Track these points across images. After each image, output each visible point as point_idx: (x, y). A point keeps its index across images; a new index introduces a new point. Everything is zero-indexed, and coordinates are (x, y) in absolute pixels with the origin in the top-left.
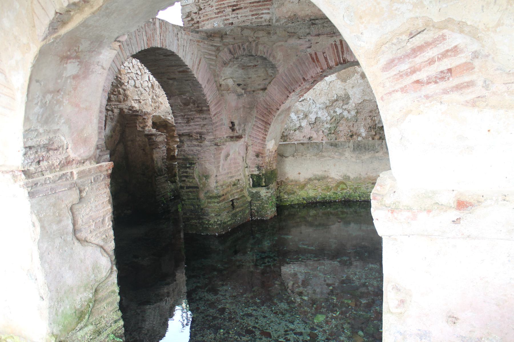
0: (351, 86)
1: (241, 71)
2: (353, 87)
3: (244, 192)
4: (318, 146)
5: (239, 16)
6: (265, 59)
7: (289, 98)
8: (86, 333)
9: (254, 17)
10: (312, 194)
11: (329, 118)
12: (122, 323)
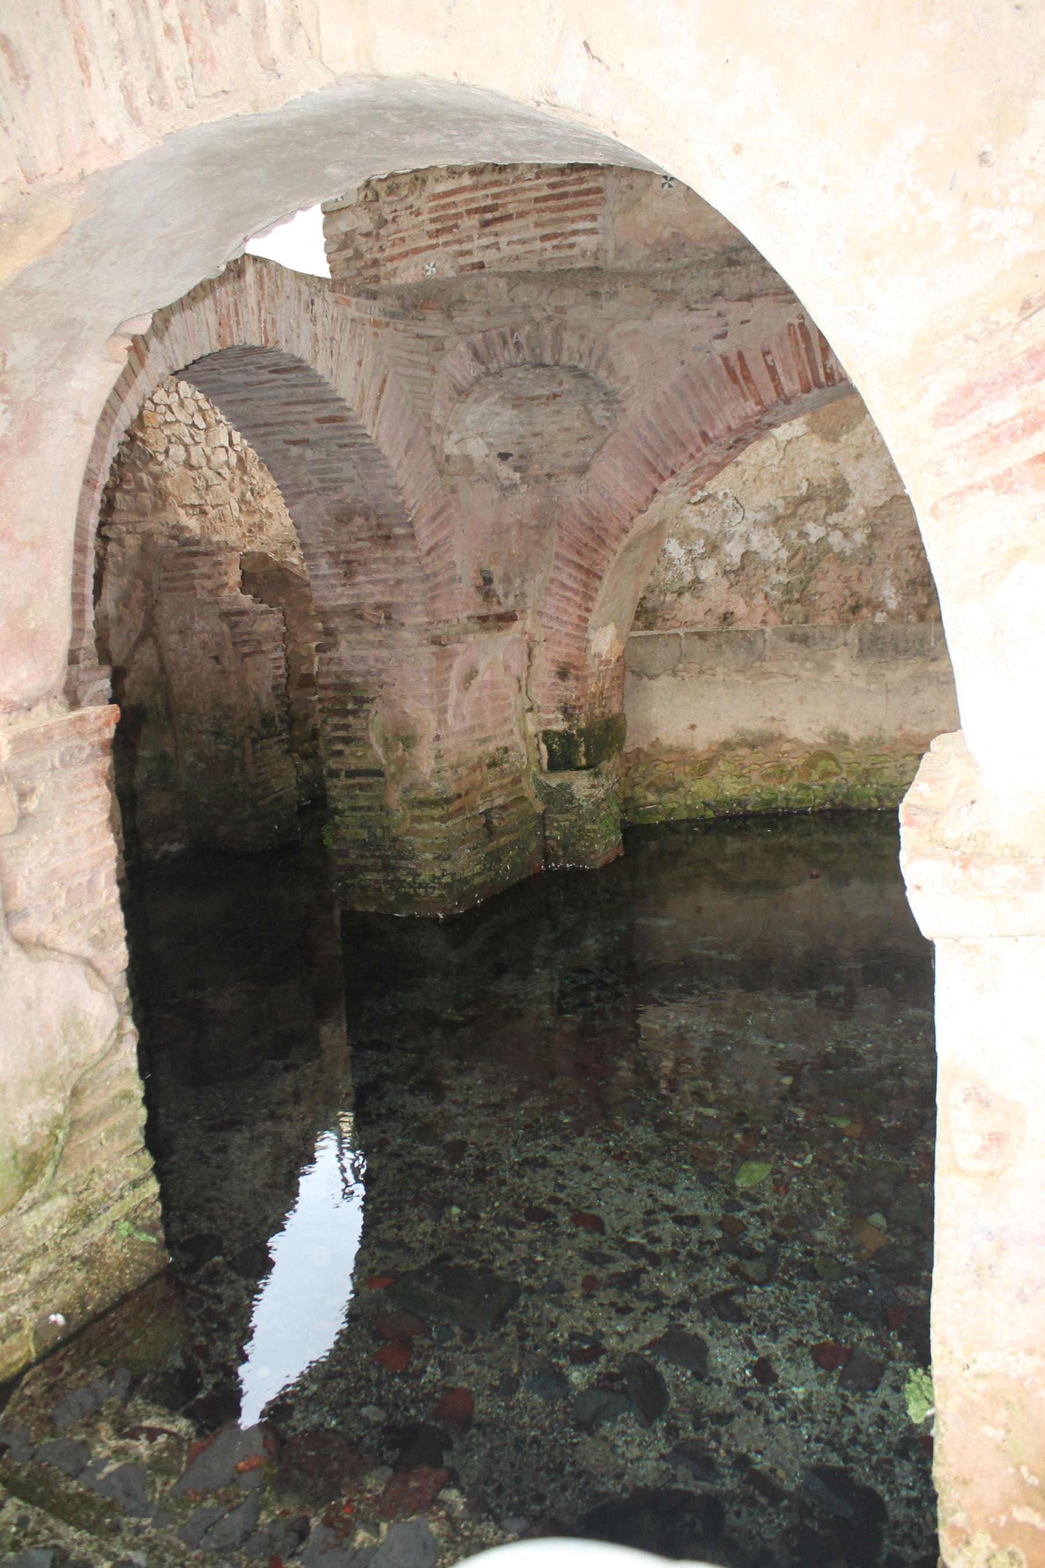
0: (853, 452)
1: (509, 414)
2: (859, 457)
3: (524, 784)
4: (751, 642)
5: (503, 240)
6: (584, 375)
7: (660, 499)
8: (49, 1220)
9: (548, 244)
10: (731, 788)
11: (784, 554)
12: (153, 1187)
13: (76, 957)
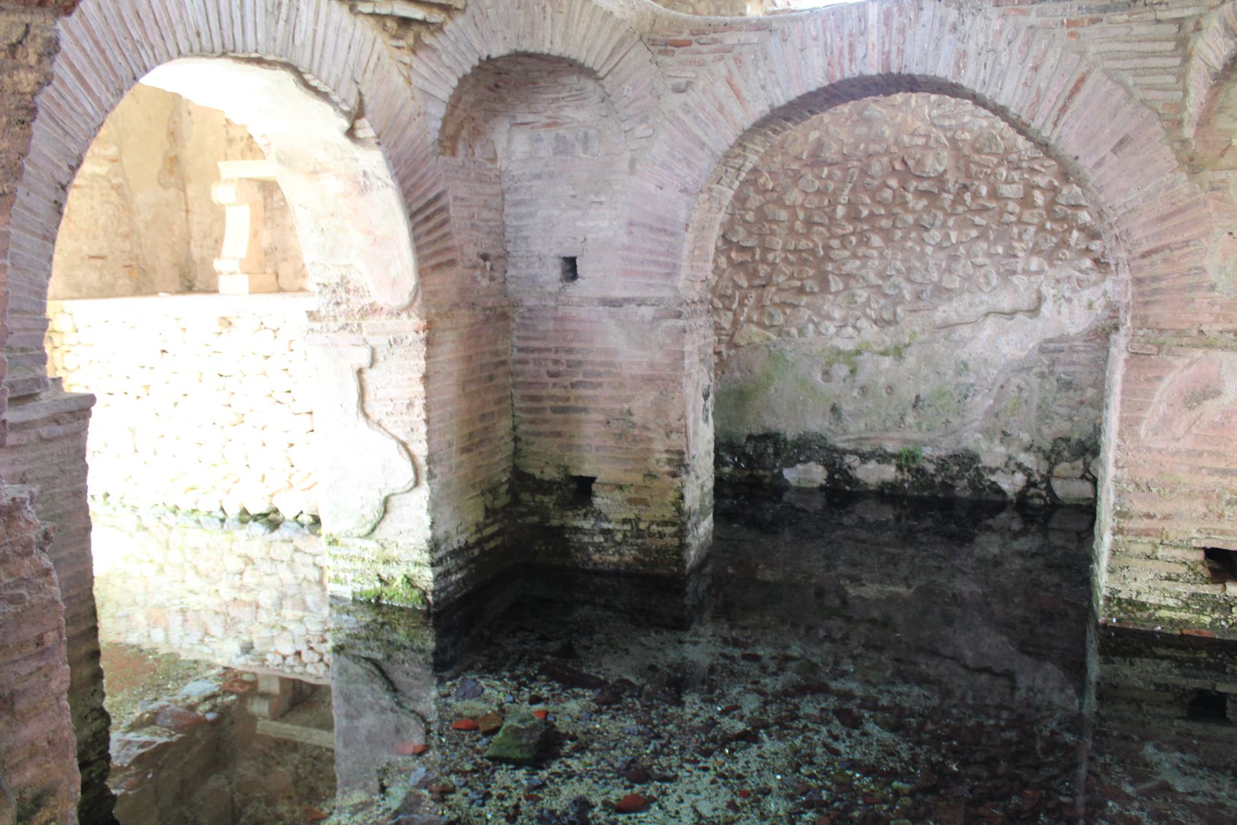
13: (394, 437)
